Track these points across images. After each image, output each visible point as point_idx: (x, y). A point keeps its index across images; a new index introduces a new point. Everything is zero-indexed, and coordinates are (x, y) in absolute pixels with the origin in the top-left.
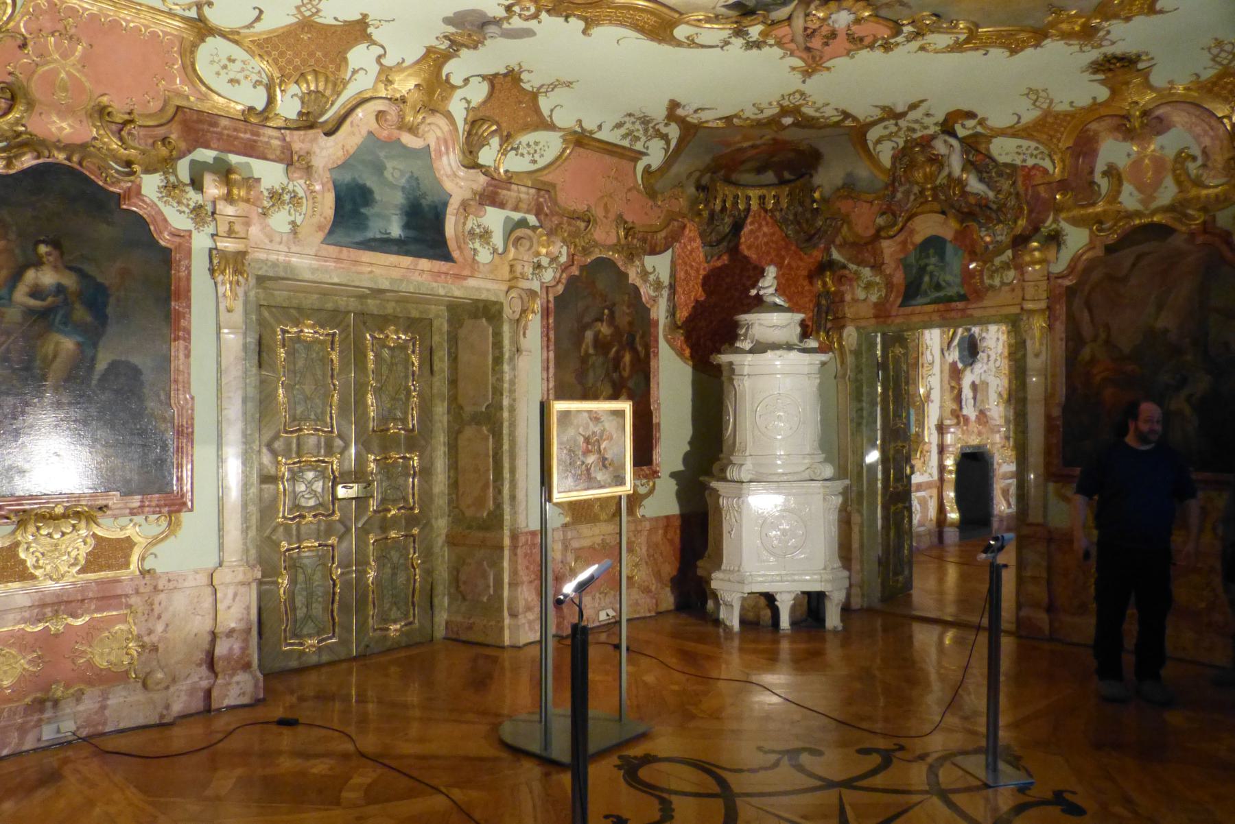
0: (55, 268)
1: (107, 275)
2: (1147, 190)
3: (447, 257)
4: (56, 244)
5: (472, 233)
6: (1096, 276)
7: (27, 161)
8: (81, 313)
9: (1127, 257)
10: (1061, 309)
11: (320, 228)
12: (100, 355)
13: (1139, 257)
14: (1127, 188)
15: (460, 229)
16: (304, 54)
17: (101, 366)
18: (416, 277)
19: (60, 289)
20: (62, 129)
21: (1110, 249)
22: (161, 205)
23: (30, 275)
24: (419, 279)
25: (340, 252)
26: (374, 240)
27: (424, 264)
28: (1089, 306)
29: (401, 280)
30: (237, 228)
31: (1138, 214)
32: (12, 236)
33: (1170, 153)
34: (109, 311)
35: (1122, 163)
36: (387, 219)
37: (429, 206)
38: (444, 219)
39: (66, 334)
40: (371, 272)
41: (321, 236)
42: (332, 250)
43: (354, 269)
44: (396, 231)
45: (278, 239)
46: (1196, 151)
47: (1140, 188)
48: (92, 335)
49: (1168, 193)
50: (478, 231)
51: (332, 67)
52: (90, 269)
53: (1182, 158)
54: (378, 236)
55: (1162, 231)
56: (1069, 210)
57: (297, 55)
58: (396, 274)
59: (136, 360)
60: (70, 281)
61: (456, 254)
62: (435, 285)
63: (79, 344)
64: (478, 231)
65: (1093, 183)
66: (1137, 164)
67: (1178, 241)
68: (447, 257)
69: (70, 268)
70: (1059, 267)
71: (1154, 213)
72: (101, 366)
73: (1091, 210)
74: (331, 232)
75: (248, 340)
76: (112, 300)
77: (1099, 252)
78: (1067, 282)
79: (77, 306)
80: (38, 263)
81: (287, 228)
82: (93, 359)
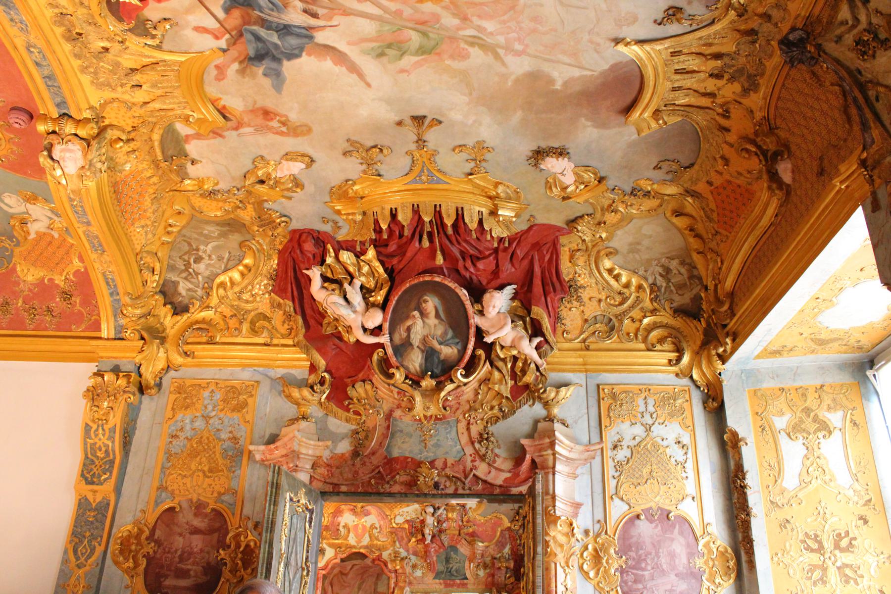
2: (359, 538)
6: (336, 571)
9: (349, 564)
10: (320, 585)
13: (353, 566)
14: (352, 535)
21: (343, 560)
28: (331, 584)
31: (354, 547)
33: (368, 525)
35: (351, 524)
46: (377, 525)
47: (357, 535)
49: (366, 541)
53: (373, 527)
55: (363, 556)
56: (328, 539)
65: (338, 530)
66: (356, 526)
67: (368, 561)
70: (321, 564)
71: (361, 548)
73: (337, 541)
77: (338, 561)
78: (324, 572)
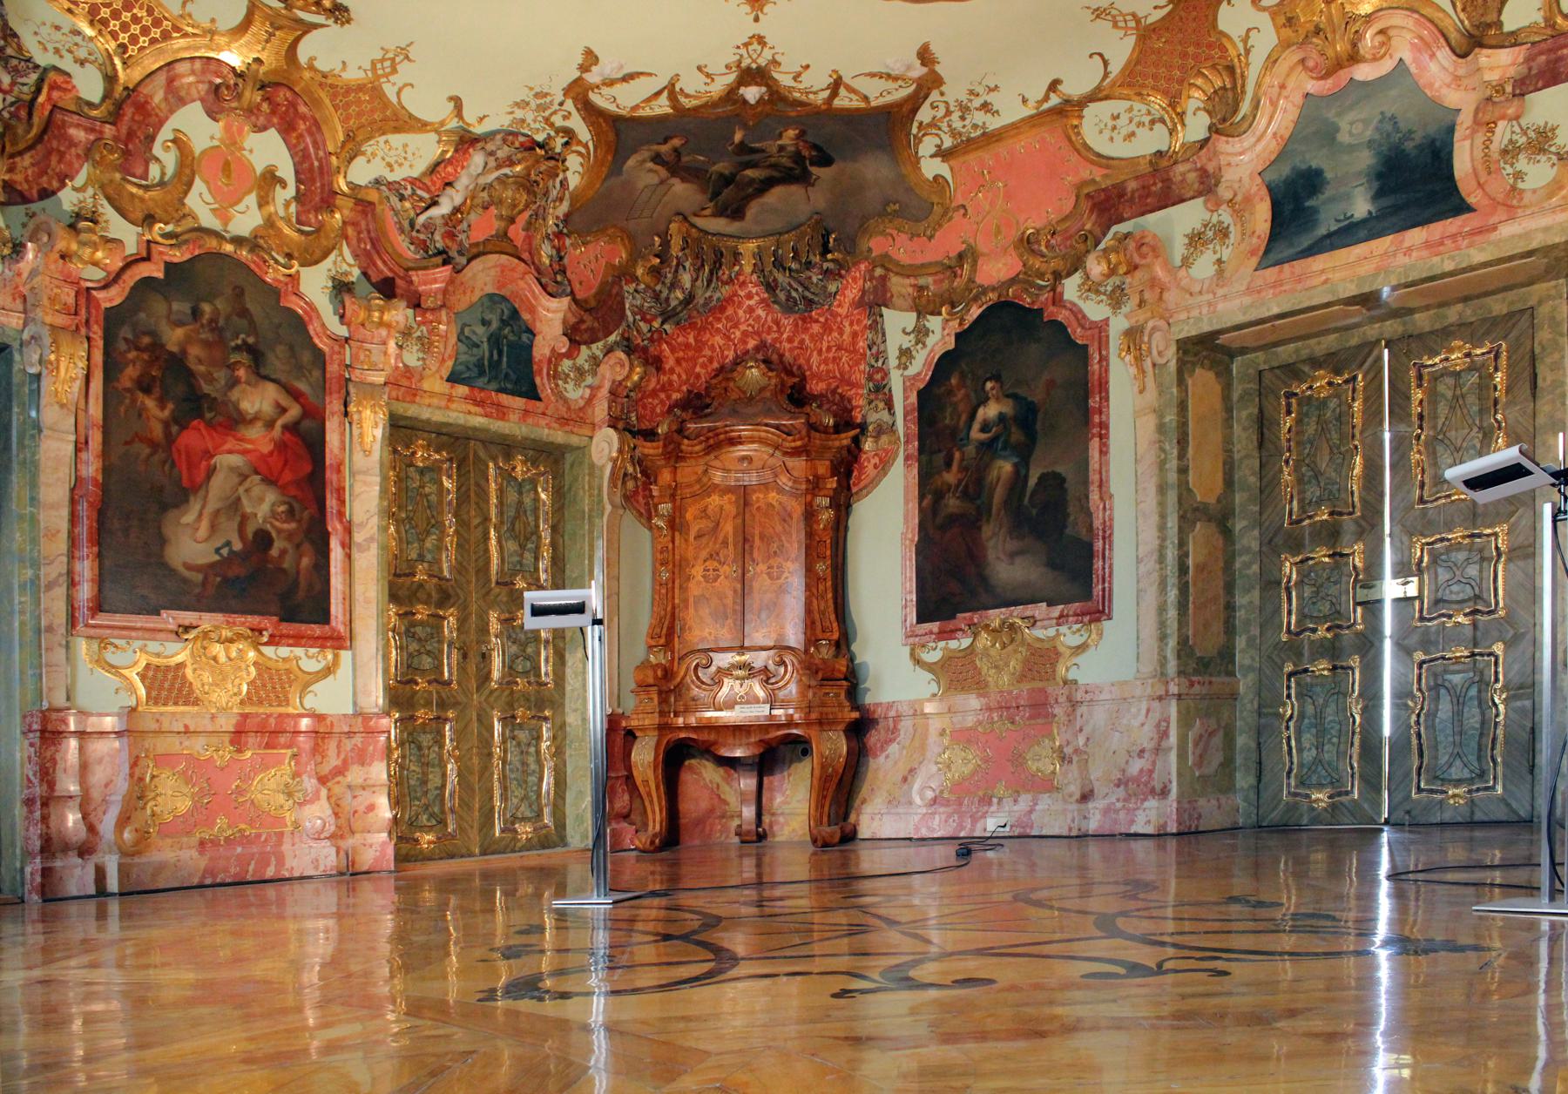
0: (997, 399)
1: (1037, 395)
3: (1462, 208)
4: (996, 378)
5: (1510, 152)
7: (975, 312)
8: (1017, 435)
11: (1253, 253)
12: (1032, 472)
15: (1479, 154)
16: (1177, 61)
17: (1032, 482)
18: (1402, 260)
19: (1002, 418)
20: (999, 270)
22: (1081, 303)
23: (981, 412)
24: (1406, 260)
25: (1281, 272)
26: (1329, 235)
27: (1416, 236)
29: (1375, 275)
30: (1147, 295)
32: (969, 382)
34: (1038, 426)
36: (1347, 197)
37: (1419, 147)
38: (1450, 153)
39: (1005, 458)
40: (1326, 281)
41: (1254, 261)
42: (1271, 274)
43: (1299, 287)
44: (1361, 207)
45: (1197, 288)
48: (1024, 455)
50: (1522, 140)
51: (1216, 53)
52: (1022, 392)
54: (1333, 228)
57: (1170, 67)
58: (1366, 269)
59: (1059, 469)
60: (1007, 407)
61: (1471, 200)
62: (1436, 259)
63: (1016, 465)
64: (1522, 140)
68: (1462, 208)
69: (1007, 396)
72: (1032, 482)
74: (1266, 252)
75: (1167, 419)
76: (1040, 416)
79: (1014, 429)
80: (984, 401)
81: (1211, 270)
82: (1026, 477)
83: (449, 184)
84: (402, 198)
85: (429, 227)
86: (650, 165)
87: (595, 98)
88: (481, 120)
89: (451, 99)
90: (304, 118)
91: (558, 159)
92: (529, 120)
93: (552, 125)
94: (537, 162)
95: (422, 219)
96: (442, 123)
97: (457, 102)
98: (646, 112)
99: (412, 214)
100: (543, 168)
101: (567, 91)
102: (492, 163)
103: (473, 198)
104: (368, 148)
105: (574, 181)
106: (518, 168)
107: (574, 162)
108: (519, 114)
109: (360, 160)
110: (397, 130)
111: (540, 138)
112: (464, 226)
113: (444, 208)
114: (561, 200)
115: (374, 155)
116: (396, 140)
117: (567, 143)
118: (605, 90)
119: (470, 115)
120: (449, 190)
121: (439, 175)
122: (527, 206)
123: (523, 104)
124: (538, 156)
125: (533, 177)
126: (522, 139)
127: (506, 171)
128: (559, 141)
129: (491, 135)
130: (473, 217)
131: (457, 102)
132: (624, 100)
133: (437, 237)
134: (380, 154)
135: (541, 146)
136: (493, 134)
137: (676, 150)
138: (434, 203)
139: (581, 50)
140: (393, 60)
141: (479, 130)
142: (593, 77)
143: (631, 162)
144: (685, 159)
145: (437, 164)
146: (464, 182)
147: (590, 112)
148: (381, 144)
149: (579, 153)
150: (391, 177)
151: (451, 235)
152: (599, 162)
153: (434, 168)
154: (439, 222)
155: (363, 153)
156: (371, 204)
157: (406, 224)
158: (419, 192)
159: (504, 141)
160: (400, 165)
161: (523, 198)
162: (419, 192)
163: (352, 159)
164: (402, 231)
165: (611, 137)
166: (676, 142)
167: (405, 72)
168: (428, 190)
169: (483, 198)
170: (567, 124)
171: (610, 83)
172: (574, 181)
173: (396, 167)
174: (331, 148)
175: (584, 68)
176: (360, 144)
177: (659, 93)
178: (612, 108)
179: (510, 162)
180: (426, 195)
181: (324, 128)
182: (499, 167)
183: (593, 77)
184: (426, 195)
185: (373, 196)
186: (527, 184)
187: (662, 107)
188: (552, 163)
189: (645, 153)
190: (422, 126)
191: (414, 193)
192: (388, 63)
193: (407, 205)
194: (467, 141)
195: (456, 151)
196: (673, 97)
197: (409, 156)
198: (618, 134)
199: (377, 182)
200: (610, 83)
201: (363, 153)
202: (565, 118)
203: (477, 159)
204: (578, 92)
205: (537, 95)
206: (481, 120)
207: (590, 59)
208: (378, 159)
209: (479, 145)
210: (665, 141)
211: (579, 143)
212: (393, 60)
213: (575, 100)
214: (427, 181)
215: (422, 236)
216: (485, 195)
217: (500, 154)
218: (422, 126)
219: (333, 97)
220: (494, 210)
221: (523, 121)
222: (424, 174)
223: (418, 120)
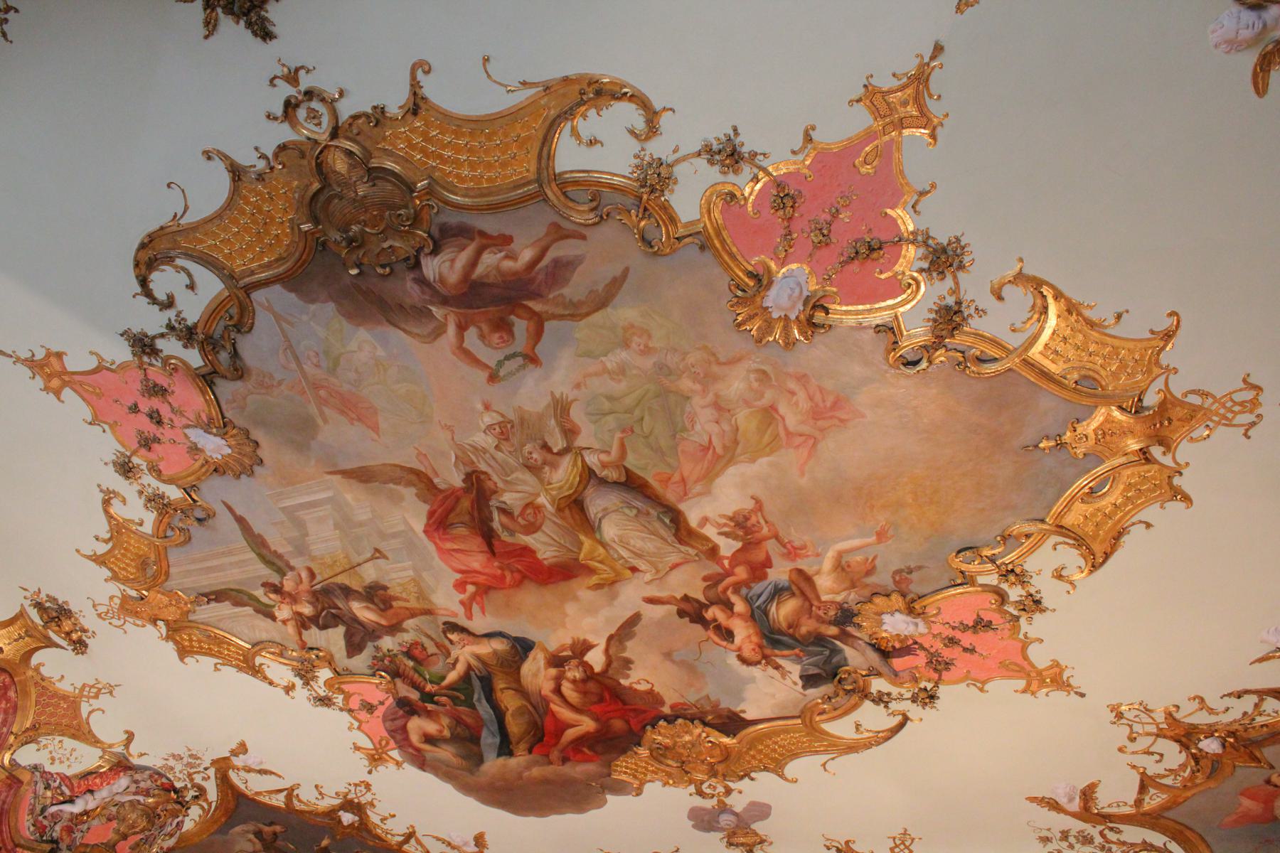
83: (91, 792)
84: (47, 787)
85: (56, 818)
86: (251, 836)
87: (232, 775)
88: (142, 755)
89: (127, 732)
90: (8, 700)
91: (185, 806)
92: (177, 770)
93: (192, 780)
94: (168, 801)
95: (54, 809)
96: (111, 746)
97: (130, 736)
98: (265, 799)
99: (48, 802)
100: (169, 807)
101: (214, 762)
102: (133, 788)
103: (104, 808)
104: (43, 740)
105: (188, 825)
106: (151, 800)
107: (195, 812)
108: (172, 762)
109: (33, 746)
110: (74, 737)
111: (178, 785)
112: (86, 826)
113: (77, 808)
114: (171, 835)
115: (45, 746)
116: (69, 743)
117: (196, 797)
118: (242, 773)
119: (134, 748)
120: (88, 796)
121: (88, 781)
122: (142, 831)
123: (178, 758)
124: (172, 796)
125: (159, 811)
126: (164, 780)
127: (141, 798)
128: (192, 793)
129: (143, 769)
130: (95, 822)
131: (130, 736)
132: (253, 785)
133: (58, 828)
134: (50, 748)
135: (176, 791)
136: (146, 768)
137: (275, 834)
138: (71, 801)
139: (238, 741)
140: (100, 690)
141: (135, 761)
142: (238, 761)
143: (238, 829)
144: (280, 843)
145: (90, 773)
146: (103, 794)
147: (224, 781)
148: (56, 742)
149: (202, 808)
150: (49, 768)
151: (69, 830)
152: (214, 820)
153: (86, 775)
154: (66, 816)
155: (38, 743)
156: (21, 782)
157: (38, 808)
158: (64, 788)
159: (151, 776)
160: (61, 762)
161: (143, 823)
162: (64, 788)
163: (27, 743)
164: (32, 812)
165: (232, 805)
166: (278, 828)
167: (104, 700)
168: (72, 790)
169: (113, 811)
170: (203, 783)
171: (249, 770)
172: (188, 825)
173: (57, 762)
174: (14, 729)
175: (234, 753)
176: (39, 736)
177: (280, 791)
178: (242, 787)
179: (147, 793)
180: (67, 792)
181: (19, 713)
182: (136, 793)
183: (238, 761)
184: (67, 792)
185: (25, 777)
186: (151, 815)
187: (279, 801)
188: (178, 807)
189: (250, 827)
190: (94, 741)
191: (59, 787)
192: (94, 690)
193: (49, 794)
194: (122, 766)
195: (110, 769)
196: (289, 797)
197: (72, 759)
198: (237, 806)
199: (36, 767)
200: (249, 770)
201: (38, 743)
202: (204, 779)
203: (123, 781)
204: (222, 767)
205: (191, 756)
206: (142, 755)
207: (242, 748)
208: (46, 751)
209: (130, 772)
210: (271, 824)
211: (206, 800)
212: (100, 690)
213: (217, 771)
214: (75, 782)
215: (45, 823)
216: (114, 809)
217: (142, 785)
218: (94, 741)
219: (40, 695)
220: (115, 824)
221: (172, 768)
222: (76, 776)
223: (94, 736)
